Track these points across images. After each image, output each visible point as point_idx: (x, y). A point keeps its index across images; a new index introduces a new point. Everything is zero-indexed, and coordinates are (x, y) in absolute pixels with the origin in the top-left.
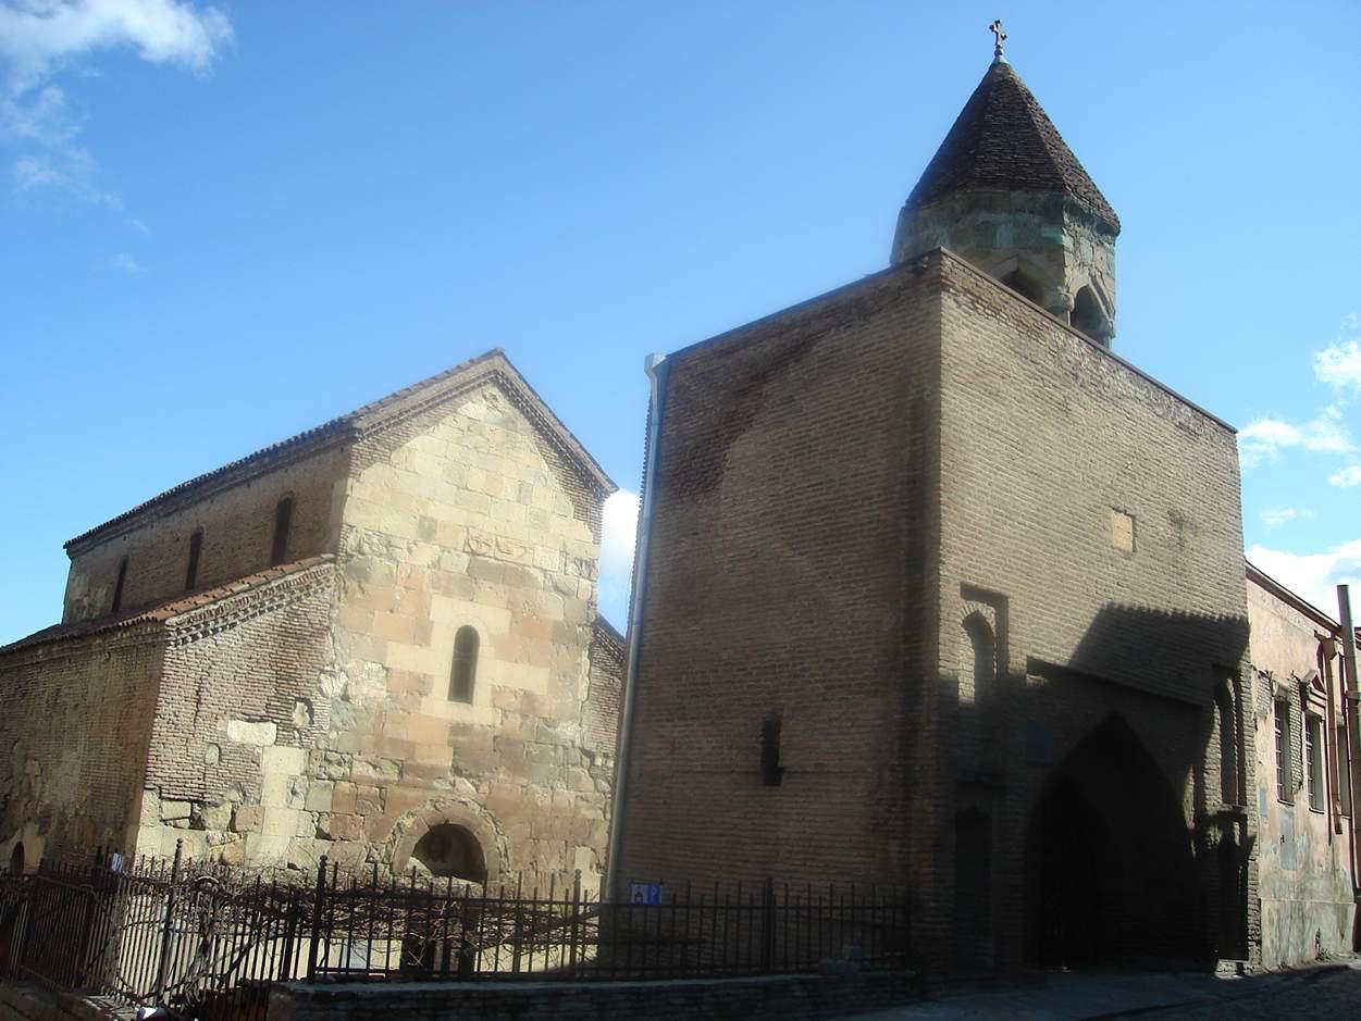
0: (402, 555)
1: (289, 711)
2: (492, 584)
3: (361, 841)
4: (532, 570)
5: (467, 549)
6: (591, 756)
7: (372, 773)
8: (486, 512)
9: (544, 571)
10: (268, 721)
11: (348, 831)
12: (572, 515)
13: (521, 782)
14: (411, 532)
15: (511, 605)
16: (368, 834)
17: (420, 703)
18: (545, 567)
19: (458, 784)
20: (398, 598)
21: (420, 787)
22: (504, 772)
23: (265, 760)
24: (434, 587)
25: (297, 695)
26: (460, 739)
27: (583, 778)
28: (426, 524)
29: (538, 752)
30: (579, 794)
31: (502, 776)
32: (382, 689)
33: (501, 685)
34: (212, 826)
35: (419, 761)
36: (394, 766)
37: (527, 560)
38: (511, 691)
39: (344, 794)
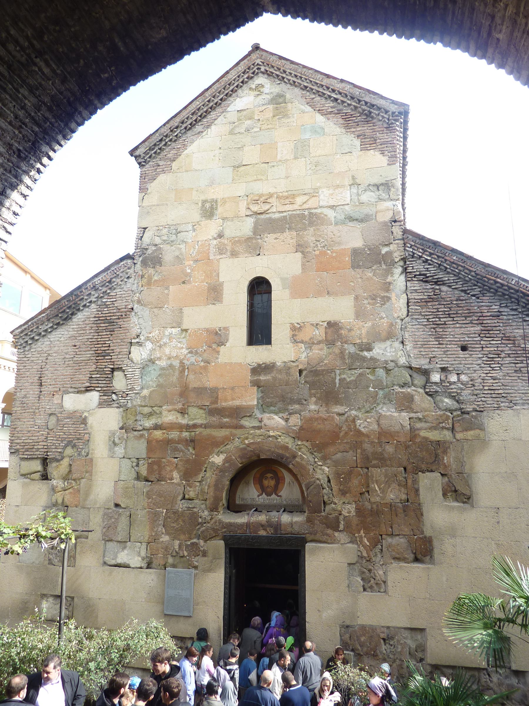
0: (189, 236)
1: (111, 379)
2: (275, 236)
3: (175, 481)
4: (319, 211)
5: (250, 213)
6: (426, 373)
7: (184, 421)
8: (263, 178)
9: (332, 207)
10: (91, 390)
11: (163, 473)
12: (359, 148)
13: (336, 410)
14: (196, 216)
15: (300, 248)
16: (182, 473)
17: (218, 352)
18: (331, 203)
19: (265, 421)
20: (189, 271)
21: (227, 427)
22: (316, 403)
23: (90, 421)
24: (221, 254)
25: (112, 367)
26: (262, 378)
27: (416, 398)
28: (208, 205)
29: (352, 378)
30: (412, 415)
31: (313, 407)
32: (183, 348)
33: (299, 321)
34: (56, 476)
35: (224, 404)
36: (202, 411)
37: (312, 203)
38: (312, 325)
39: (158, 441)
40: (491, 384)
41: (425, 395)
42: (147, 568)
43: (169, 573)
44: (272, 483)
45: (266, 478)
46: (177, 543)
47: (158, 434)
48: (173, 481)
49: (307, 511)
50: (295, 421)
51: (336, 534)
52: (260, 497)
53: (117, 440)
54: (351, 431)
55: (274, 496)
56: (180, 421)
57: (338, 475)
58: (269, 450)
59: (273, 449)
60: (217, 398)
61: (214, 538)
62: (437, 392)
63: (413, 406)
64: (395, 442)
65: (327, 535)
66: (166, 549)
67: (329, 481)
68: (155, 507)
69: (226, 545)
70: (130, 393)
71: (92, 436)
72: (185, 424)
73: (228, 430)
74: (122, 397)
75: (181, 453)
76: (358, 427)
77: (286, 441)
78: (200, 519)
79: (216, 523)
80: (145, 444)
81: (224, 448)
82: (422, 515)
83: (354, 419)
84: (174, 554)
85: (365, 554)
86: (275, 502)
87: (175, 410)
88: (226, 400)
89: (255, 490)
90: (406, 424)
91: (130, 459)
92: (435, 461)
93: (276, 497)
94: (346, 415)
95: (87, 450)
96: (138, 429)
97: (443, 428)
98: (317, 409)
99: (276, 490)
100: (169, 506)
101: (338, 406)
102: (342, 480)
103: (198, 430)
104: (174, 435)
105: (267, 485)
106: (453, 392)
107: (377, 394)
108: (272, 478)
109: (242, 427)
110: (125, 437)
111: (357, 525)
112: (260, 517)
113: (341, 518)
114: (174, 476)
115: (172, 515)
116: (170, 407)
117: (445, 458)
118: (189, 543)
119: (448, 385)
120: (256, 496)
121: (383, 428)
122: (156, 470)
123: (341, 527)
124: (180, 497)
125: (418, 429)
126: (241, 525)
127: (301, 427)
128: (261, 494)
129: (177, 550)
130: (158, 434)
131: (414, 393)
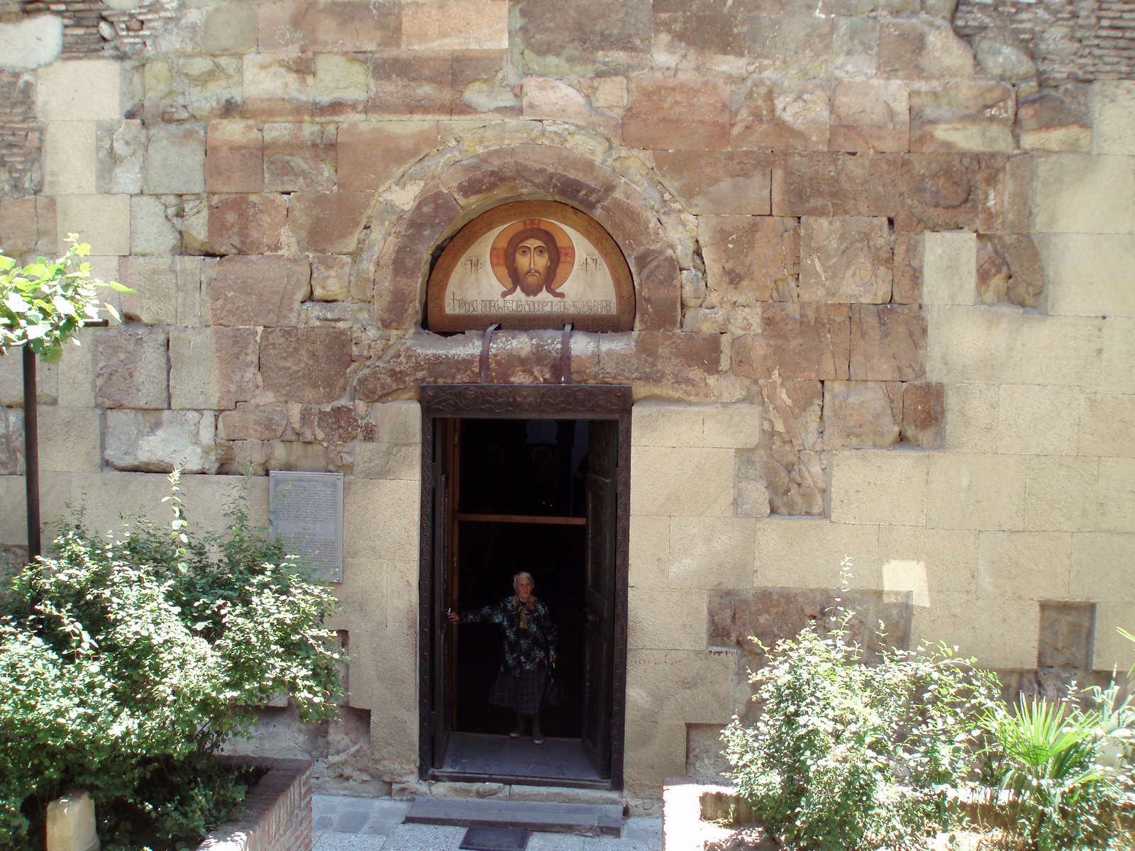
3: (283, 252)
11: (254, 234)
13: (724, 68)
16: (304, 234)
21: (426, 110)
22: (671, 49)
23: (43, 95)
39: (234, 148)
40: (1118, 15)
41: (951, 33)
42: (218, 473)
43: (278, 482)
44: (541, 262)
45: (526, 251)
46: (295, 410)
47: (234, 130)
48: (280, 253)
49: (638, 325)
50: (613, 94)
51: (712, 380)
52: (509, 297)
53: (120, 148)
54: (761, 121)
55: (544, 295)
56: (295, 94)
57: (722, 236)
58: (542, 171)
59: (551, 170)
60: (398, 30)
61: (395, 395)
62: (983, 28)
63: (924, 62)
64: (871, 151)
65: (688, 381)
66: (268, 424)
67: (698, 253)
68: (233, 320)
69: (426, 411)
70: (150, 17)
71: (48, 138)
72: (306, 103)
73: (429, 117)
74: (128, 29)
75: (301, 179)
76: (778, 112)
77: (587, 146)
78: (354, 348)
79: (399, 356)
80: (200, 156)
81: (418, 167)
82: (924, 331)
83: (770, 93)
84: (290, 436)
85: (780, 427)
86: (548, 309)
87: (282, 64)
88: (423, 37)
89: (494, 281)
90: (901, 107)
91: (158, 196)
92: (966, 201)
93: (551, 297)
94: (749, 83)
95: (36, 176)
96: (177, 117)
97: (992, 119)
98: (673, 65)
99: (550, 280)
100: (273, 317)
101: (731, 58)
102: (730, 246)
103: (348, 119)
104: (277, 130)
105: (526, 268)
106: (1024, 31)
107: (833, 27)
108: (541, 251)
109: (467, 109)
110: (143, 139)
111: (765, 357)
112: (515, 342)
113: (725, 340)
114: (283, 239)
115: (282, 340)
116: (266, 57)
117: (992, 196)
118: (328, 409)
119: (1013, 10)
120: (497, 297)
121: (843, 115)
122: (232, 226)
123: (724, 364)
124: (301, 293)
125: (933, 122)
126: (464, 360)
127: (629, 109)
128: (512, 290)
129: (297, 426)
130: (234, 130)
131: (926, 28)
